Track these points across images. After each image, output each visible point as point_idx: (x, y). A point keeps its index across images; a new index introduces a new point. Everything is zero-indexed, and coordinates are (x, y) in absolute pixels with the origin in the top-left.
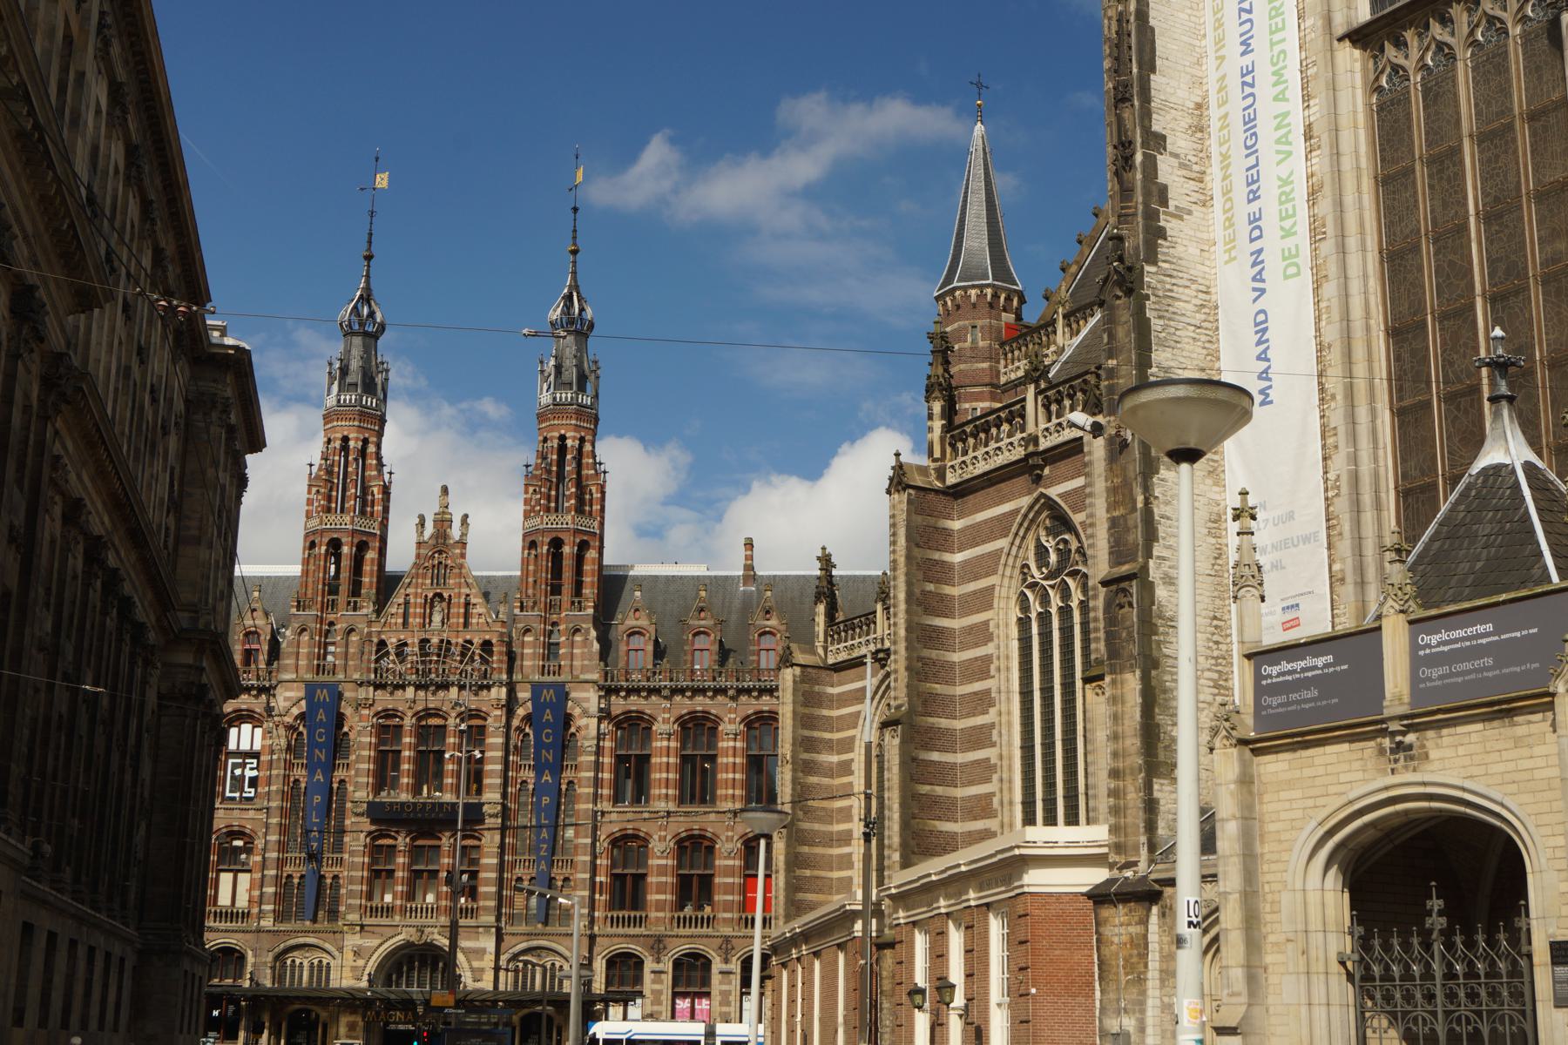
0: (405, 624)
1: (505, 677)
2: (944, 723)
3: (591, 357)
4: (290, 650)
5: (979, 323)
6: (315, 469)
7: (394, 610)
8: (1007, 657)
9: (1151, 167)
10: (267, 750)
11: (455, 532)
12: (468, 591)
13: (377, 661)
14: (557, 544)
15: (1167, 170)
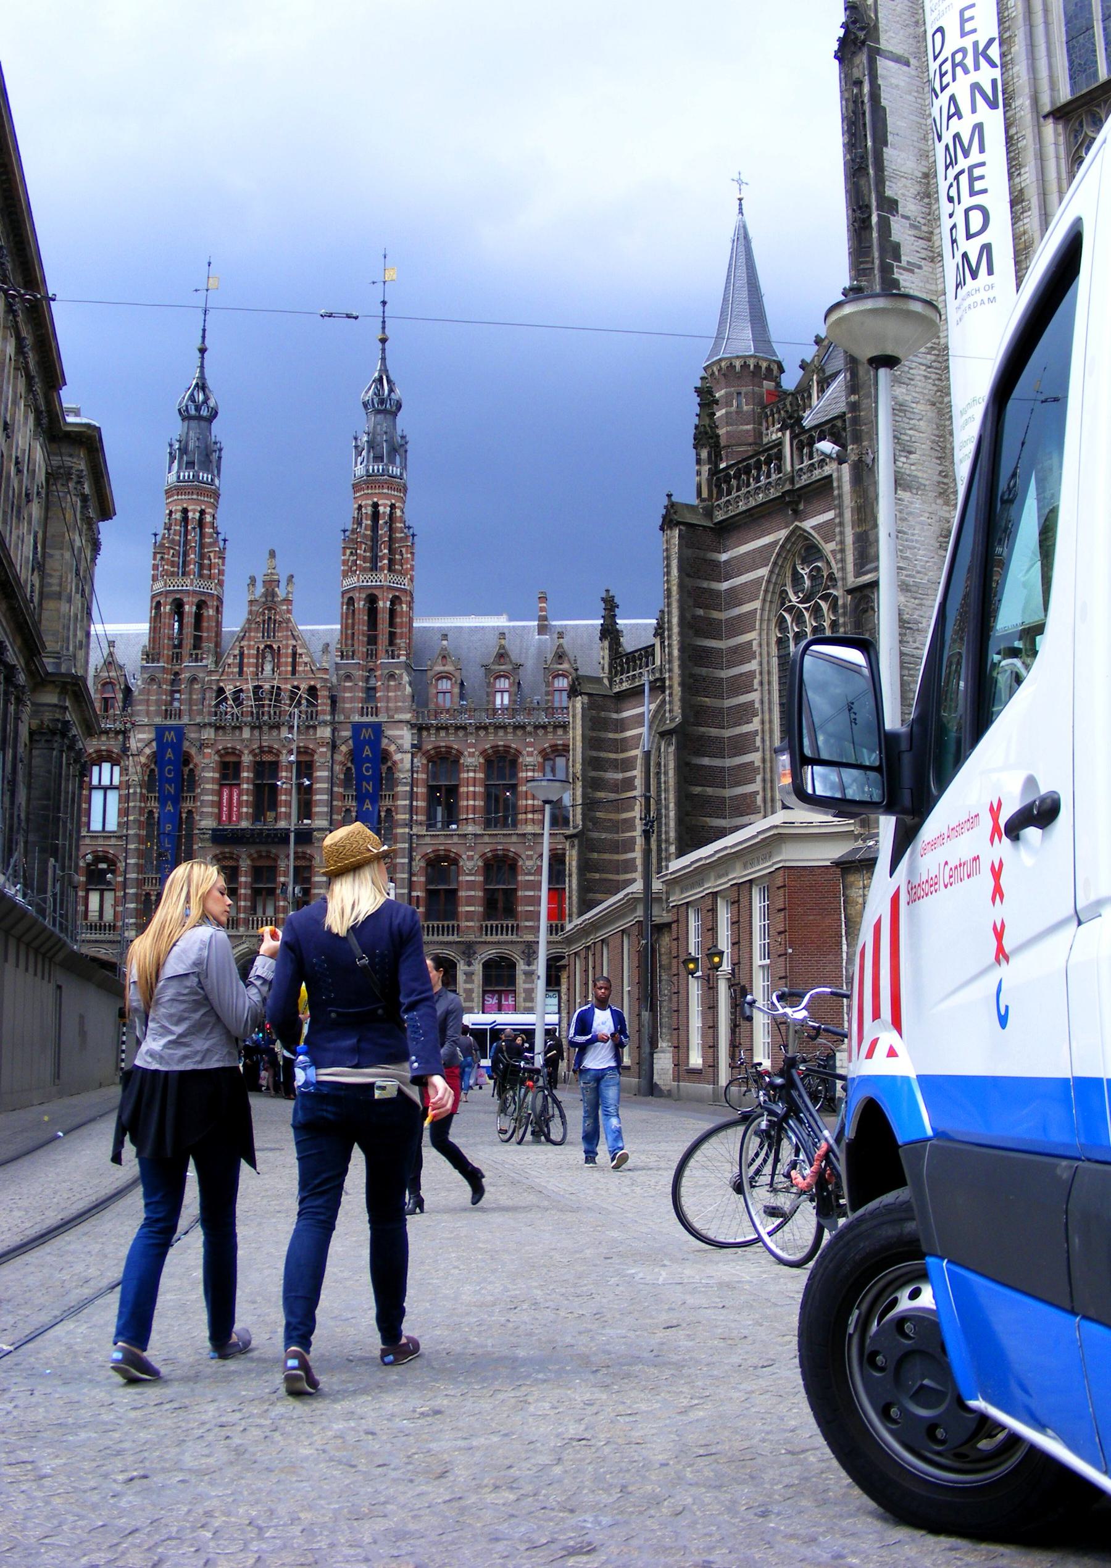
1: (328, 718)
2: (714, 732)
3: (399, 432)
5: (744, 390)
6: (159, 538)
7: (230, 661)
8: (769, 673)
9: (885, 227)
10: (124, 786)
11: (281, 593)
12: (294, 643)
13: (217, 705)
14: (372, 600)
15: (900, 231)
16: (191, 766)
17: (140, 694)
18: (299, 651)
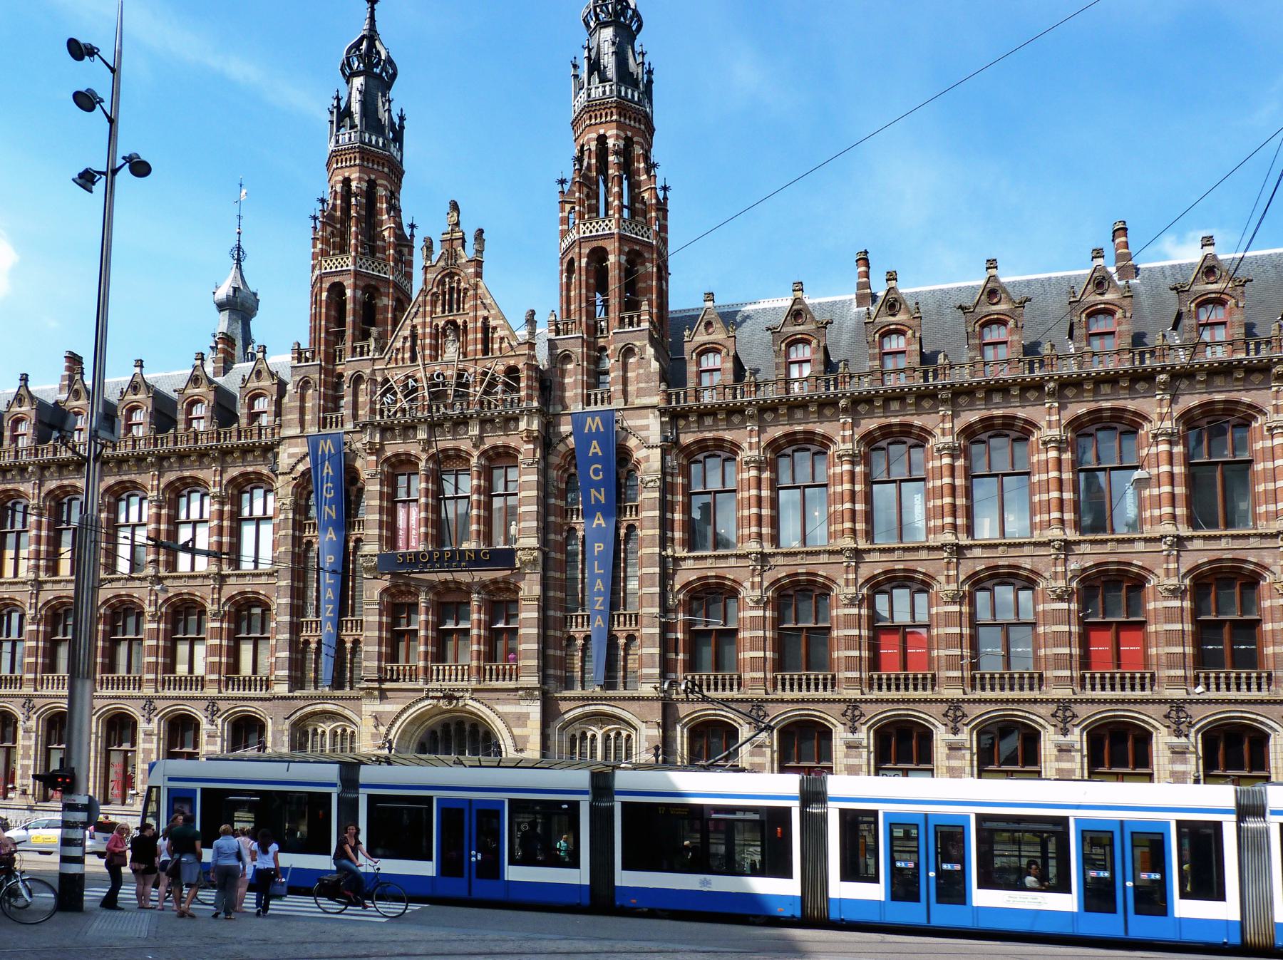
4: (293, 404)
7: (399, 344)
12: (484, 313)
16: (359, 485)
17: (290, 401)
18: (492, 323)
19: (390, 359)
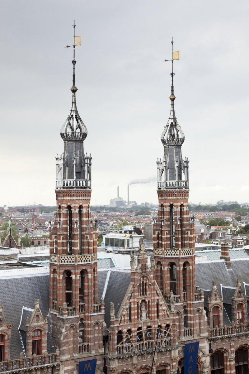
0: (130, 320)
3: (184, 159)
17: (64, 339)
19: (121, 320)
